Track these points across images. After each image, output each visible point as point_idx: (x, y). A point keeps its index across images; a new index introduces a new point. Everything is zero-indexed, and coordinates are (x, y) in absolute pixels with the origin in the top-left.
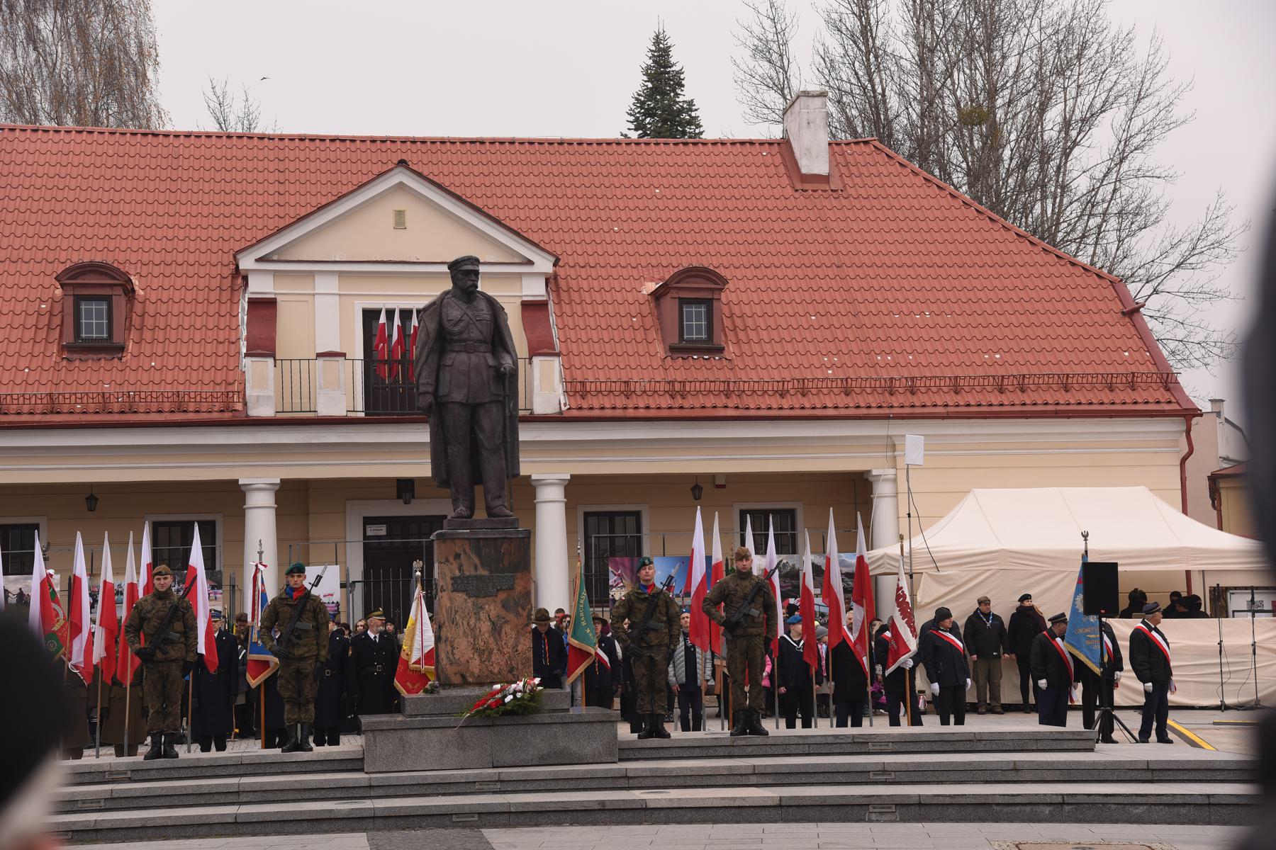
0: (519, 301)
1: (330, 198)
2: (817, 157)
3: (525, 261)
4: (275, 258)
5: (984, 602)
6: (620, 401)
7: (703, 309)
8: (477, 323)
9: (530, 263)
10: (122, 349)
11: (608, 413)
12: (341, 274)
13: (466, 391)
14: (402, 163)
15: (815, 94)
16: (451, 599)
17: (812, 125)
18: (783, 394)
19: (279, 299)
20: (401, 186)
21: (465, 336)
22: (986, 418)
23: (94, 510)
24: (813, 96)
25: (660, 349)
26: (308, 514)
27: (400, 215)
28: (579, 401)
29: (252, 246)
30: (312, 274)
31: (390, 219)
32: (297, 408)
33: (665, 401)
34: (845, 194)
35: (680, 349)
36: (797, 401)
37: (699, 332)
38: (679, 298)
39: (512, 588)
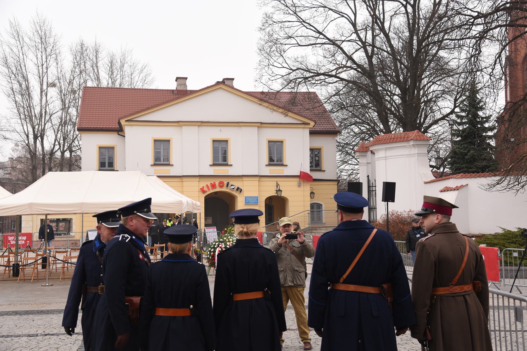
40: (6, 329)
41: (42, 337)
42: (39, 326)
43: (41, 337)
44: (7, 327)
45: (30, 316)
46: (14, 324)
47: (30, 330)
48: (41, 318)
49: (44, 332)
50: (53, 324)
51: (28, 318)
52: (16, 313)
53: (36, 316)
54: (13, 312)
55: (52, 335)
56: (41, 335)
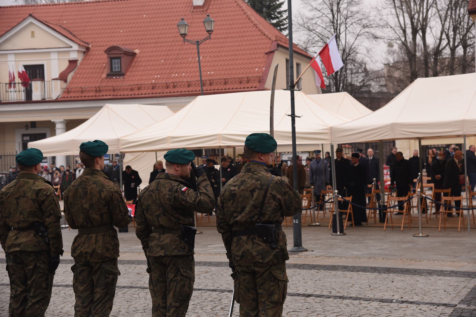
0: (67, 60)
3: (69, 46)
6: (112, 93)
7: (119, 61)
9: (71, 47)
11: (72, 99)
12: (15, 54)
14: (30, 15)
18: (132, 90)
22: (190, 96)
25: (104, 75)
27: (33, 33)
28: (66, 95)
30: (7, 54)
31: (30, 34)
33: (93, 94)
36: (136, 92)
37: (118, 69)
40: (356, 289)
41: (398, 304)
42: (397, 290)
43: (396, 305)
44: (359, 286)
45: (392, 275)
46: (368, 284)
47: (385, 293)
48: (403, 279)
49: (402, 298)
50: (417, 288)
51: (387, 278)
52: (374, 270)
53: (398, 276)
54: (372, 268)
55: (411, 303)
56: (397, 301)
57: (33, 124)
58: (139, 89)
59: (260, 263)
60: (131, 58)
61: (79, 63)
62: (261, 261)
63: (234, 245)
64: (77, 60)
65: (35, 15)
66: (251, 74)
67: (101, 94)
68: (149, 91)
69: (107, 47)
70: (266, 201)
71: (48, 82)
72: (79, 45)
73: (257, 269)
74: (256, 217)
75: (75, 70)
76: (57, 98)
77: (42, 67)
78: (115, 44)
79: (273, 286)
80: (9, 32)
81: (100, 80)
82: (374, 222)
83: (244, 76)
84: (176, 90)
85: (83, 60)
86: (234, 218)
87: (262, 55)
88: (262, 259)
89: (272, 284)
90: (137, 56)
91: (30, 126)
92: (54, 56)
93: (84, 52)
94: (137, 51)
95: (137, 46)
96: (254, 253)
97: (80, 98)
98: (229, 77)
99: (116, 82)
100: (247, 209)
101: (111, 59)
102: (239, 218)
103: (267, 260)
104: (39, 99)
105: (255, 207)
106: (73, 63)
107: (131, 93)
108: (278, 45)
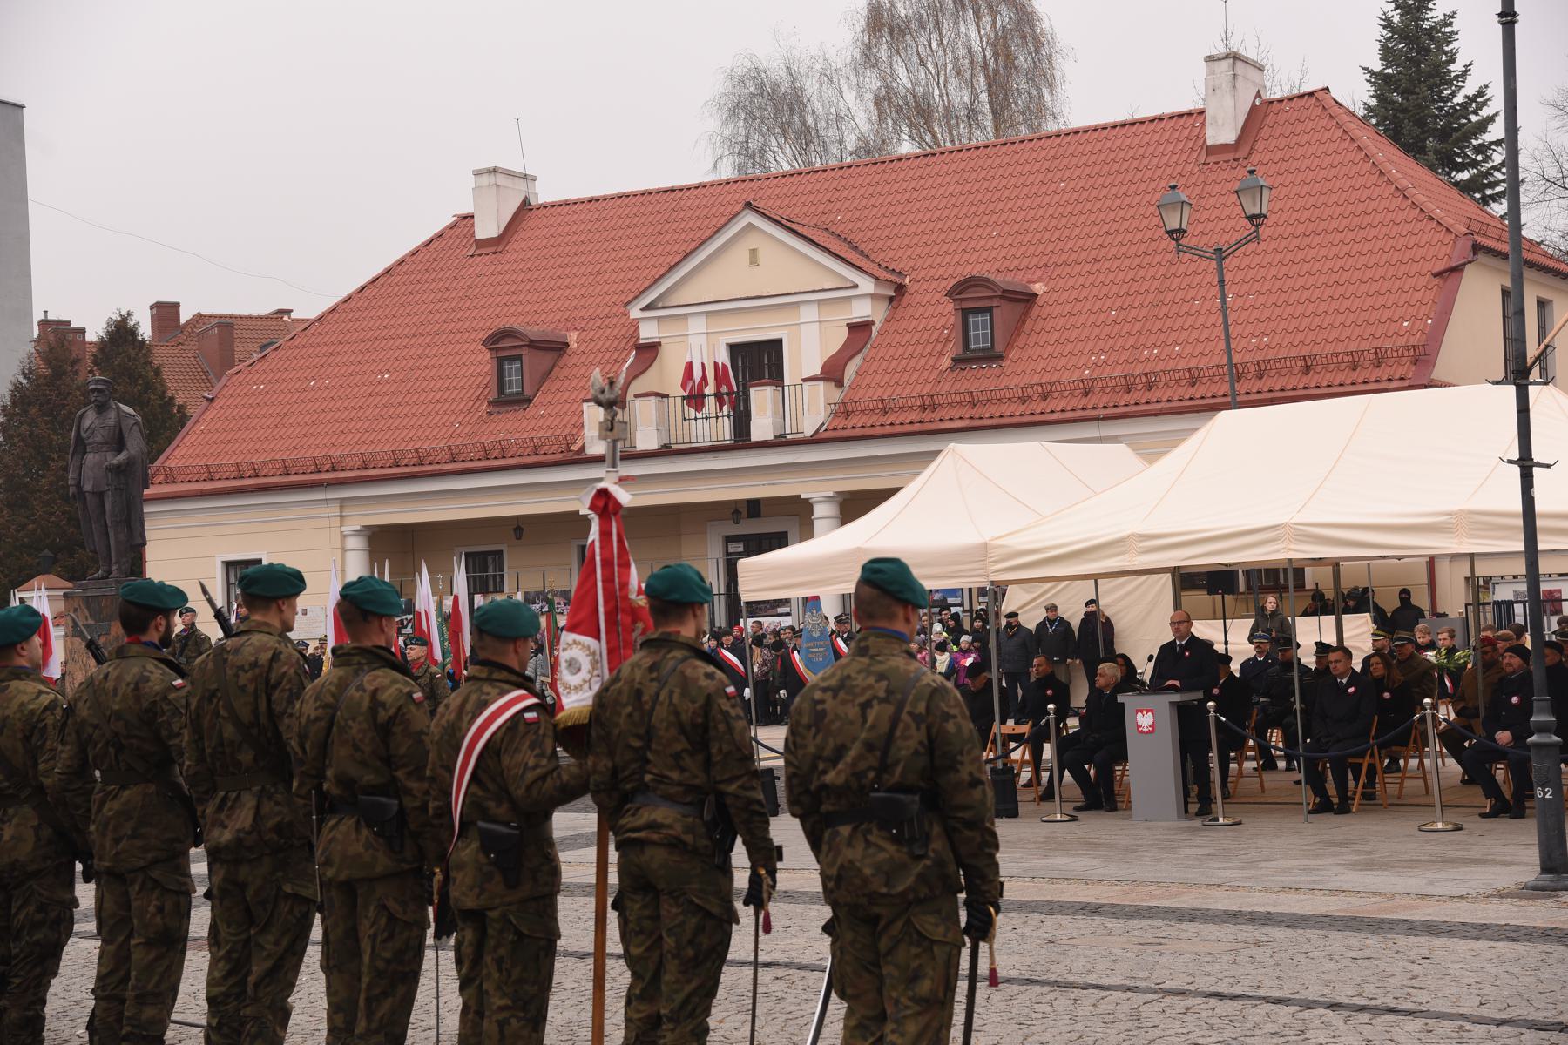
1: (693, 246)
2: (1223, 125)
3: (849, 285)
4: (660, 305)
5: (1052, 608)
8: (102, 431)
9: (856, 286)
10: (530, 401)
11: (858, 432)
13: (92, 483)
14: (748, 205)
15: (1220, 57)
16: (72, 643)
17: (1217, 91)
18: (1023, 400)
19: (663, 341)
20: (750, 226)
21: (91, 440)
22: (1198, 412)
23: (520, 538)
24: (1219, 60)
25: (946, 362)
26: (680, 535)
27: (753, 252)
28: (840, 423)
29: (636, 297)
30: (685, 316)
32: (687, 440)
33: (913, 416)
34: (1246, 162)
35: (966, 359)
38: (962, 309)
39: (108, 634)
57: (754, 508)
58: (1044, 397)
59: (883, 895)
60: (1020, 307)
61: (874, 329)
62: (884, 890)
63: (825, 848)
64: (873, 323)
65: (760, 204)
66: (1248, 354)
67: (936, 415)
68: (1074, 403)
69: (954, 282)
70: (898, 733)
71: (792, 388)
72: (877, 278)
73: (876, 910)
74: (872, 775)
75: (865, 351)
76: (817, 432)
77: (777, 344)
78: (976, 271)
79: (917, 956)
80: (693, 255)
81: (935, 374)
82: (1396, 793)
83: (1364, 345)
84: (1155, 394)
85: (887, 321)
86: (819, 779)
87: (1423, 281)
88: (886, 885)
89: (914, 950)
90: (1040, 301)
91: (745, 513)
92: (809, 314)
93: (891, 299)
94: (1038, 288)
95: (1039, 273)
96: (868, 871)
97: (879, 430)
98: (1317, 350)
99: (979, 380)
100: (852, 753)
101: (966, 313)
102: (830, 777)
103: (900, 888)
104: (770, 437)
105: (869, 746)
106: (859, 329)
107: (1022, 408)
108: (1477, 248)
